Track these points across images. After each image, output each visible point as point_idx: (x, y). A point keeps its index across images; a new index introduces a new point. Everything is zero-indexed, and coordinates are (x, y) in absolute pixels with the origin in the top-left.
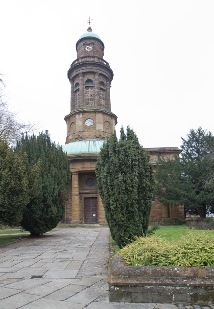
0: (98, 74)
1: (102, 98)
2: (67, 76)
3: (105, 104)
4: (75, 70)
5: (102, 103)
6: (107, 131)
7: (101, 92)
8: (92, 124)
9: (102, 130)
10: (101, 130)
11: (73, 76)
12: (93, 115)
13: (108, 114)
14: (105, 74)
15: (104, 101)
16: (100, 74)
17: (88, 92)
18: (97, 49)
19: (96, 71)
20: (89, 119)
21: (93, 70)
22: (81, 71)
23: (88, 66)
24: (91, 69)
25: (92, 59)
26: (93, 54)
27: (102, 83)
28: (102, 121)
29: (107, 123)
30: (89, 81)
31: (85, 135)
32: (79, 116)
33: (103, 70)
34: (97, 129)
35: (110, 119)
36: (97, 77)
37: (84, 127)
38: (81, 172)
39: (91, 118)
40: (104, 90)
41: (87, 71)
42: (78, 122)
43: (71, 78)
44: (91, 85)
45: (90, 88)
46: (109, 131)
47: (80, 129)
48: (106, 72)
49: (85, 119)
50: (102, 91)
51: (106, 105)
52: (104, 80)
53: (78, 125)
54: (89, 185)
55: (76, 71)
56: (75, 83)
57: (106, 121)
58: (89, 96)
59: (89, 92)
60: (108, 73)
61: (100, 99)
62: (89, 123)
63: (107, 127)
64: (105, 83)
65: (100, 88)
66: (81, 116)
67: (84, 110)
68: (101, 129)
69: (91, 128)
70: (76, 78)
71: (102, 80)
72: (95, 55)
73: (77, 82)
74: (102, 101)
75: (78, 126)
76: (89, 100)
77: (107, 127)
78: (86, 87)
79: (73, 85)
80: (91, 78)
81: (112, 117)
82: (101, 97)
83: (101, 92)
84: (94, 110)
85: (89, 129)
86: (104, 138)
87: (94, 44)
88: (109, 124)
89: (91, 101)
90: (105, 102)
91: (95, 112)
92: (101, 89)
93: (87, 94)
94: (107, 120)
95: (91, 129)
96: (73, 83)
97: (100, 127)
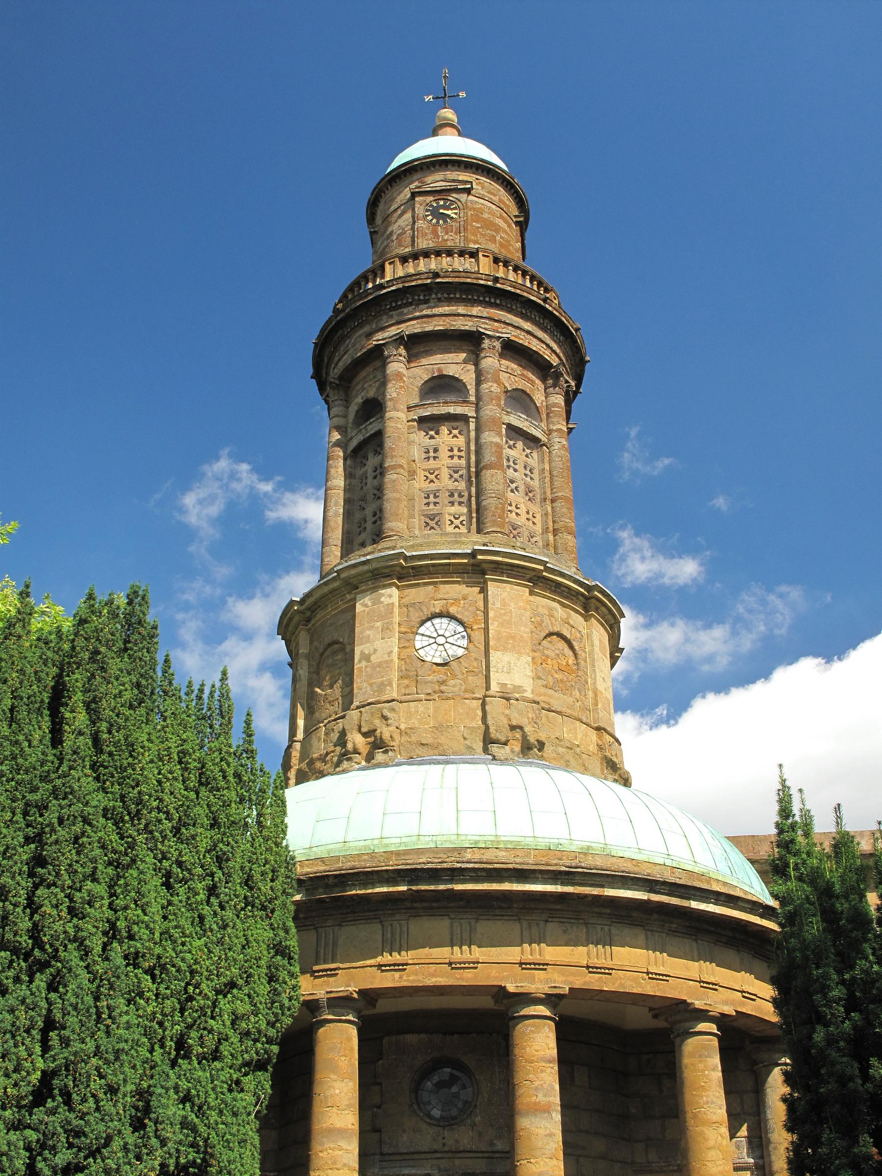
0: (498, 345)
1: (522, 488)
2: (311, 371)
3: (538, 528)
4: (361, 325)
5: (521, 521)
6: (558, 700)
7: (512, 453)
8: (460, 652)
9: (529, 695)
10: (518, 689)
11: (347, 360)
12: (463, 589)
13: (559, 585)
14: (535, 345)
15: (535, 508)
16: (511, 349)
17: (436, 450)
18: (486, 216)
19: (485, 327)
20: (440, 615)
21: (468, 325)
22: (393, 331)
23: (439, 300)
24: (459, 315)
25: (460, 264)
26: (466, 239)
27: (520, 399)
28: (525, 631)
29: (562, 645)
30: (442, 385)
31: (414, 722)
32: (377, 602)
33: (527, 326)
34: (494, 688)
35: (577, 619)
36: (491, 361)
37: (413, 668)
38: (383, 1006)
39: (453, 610)
40: (532, 441)
41: (429, 328)
42: (368, 639)
43: (335, 372)
44: (452, 409)
45: (444, 430)
46: (571, 700)
47: (382, 687)
48: (540, 334)
49: (416, 617)
50: (520, 445)
51: (545, 531)
52: (532, 383)
53: (367, 658)
54: (436, 1113)
55: (366, 329)
56: (359, 400)
57: (551, 634)
58: (445, 473)
59: (444, 453)
60: (555, 347)
61: (510, 495)
62: (439, 641)
63: (559, 676)
64: (539, 398)
65: (510, 427)
66: (391, 595)
67: (406, 558)
68: (517, 683)
69: (454, 676)
70: (363, 374)
71: (522, 385)
72: (473, 246)
73: (371, 394)
74: (522, 510)
75: (364, 663)
76: (444, 498)
77: (559, 676)
78: (422, 420)
79: (345, 416)
80: (451, 371)
81: (586, 608)
82: (512, 482)
83: (512, 453)
84: (474, 554)
85: (443, 683)
86: (541, 745)
87: (468, 191)
88: (568, 651)
89: (452, 503)
90: (538, 516)
91: (476, 570)
92: (514, 432)
93: (432, 463)
94: (556, 629)
95: (454, 686)
96: (347, 402)
97: (513, 670)
